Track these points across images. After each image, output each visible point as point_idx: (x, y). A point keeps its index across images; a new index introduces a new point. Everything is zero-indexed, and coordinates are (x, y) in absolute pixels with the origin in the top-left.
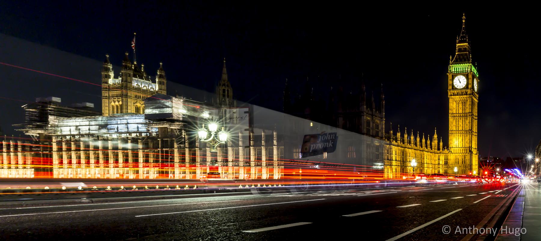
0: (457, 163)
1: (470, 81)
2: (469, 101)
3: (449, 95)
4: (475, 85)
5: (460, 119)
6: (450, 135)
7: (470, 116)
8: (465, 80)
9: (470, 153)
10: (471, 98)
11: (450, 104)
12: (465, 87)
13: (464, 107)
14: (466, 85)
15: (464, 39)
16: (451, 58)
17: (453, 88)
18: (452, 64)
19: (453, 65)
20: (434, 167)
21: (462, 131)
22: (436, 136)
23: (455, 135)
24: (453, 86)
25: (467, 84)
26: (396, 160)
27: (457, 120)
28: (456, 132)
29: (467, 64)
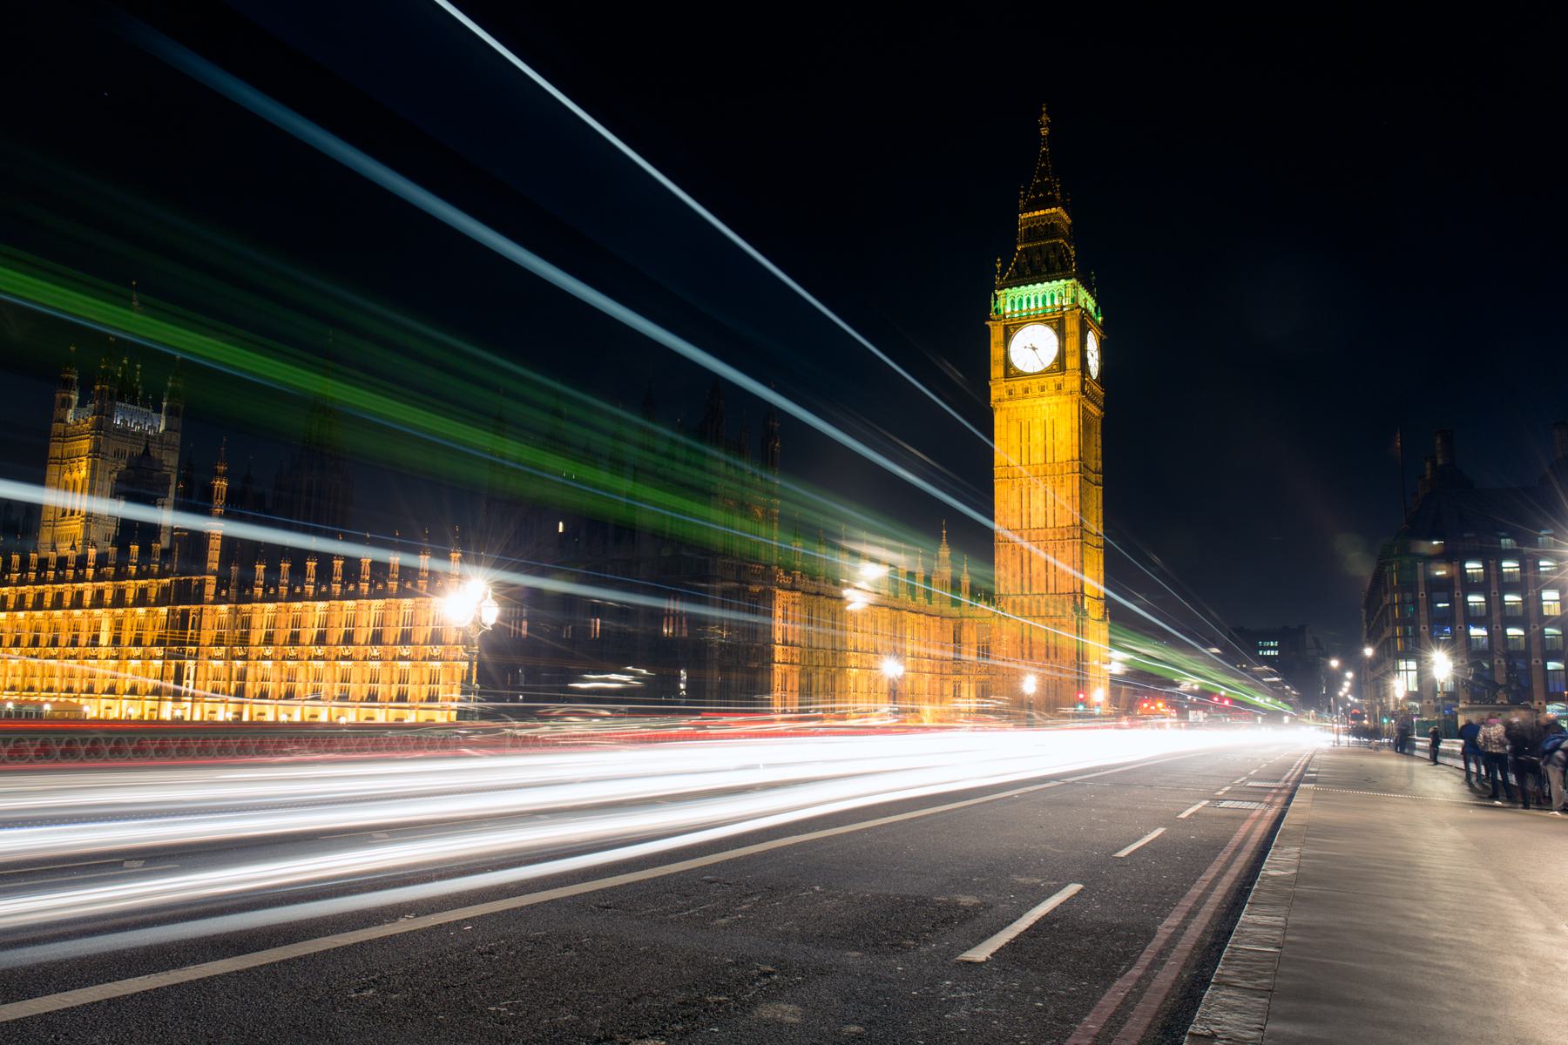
0: (1026, 656)
1: (1072, 343)
3: (993, 398)
4: (1089, 355)
6: (998, 546)
12: (1052, 365)
13: (1049, 438)
14: (1056, 360)
15: (1045, 194)
16: (999, 266)
17: (1010, 371)
19: (1007, 290)
20: (938, 671)
24: (1008, 364)
25: (1059, 352)
26: (785, 643)
27: (1025, 492)
29: (1058, 280)
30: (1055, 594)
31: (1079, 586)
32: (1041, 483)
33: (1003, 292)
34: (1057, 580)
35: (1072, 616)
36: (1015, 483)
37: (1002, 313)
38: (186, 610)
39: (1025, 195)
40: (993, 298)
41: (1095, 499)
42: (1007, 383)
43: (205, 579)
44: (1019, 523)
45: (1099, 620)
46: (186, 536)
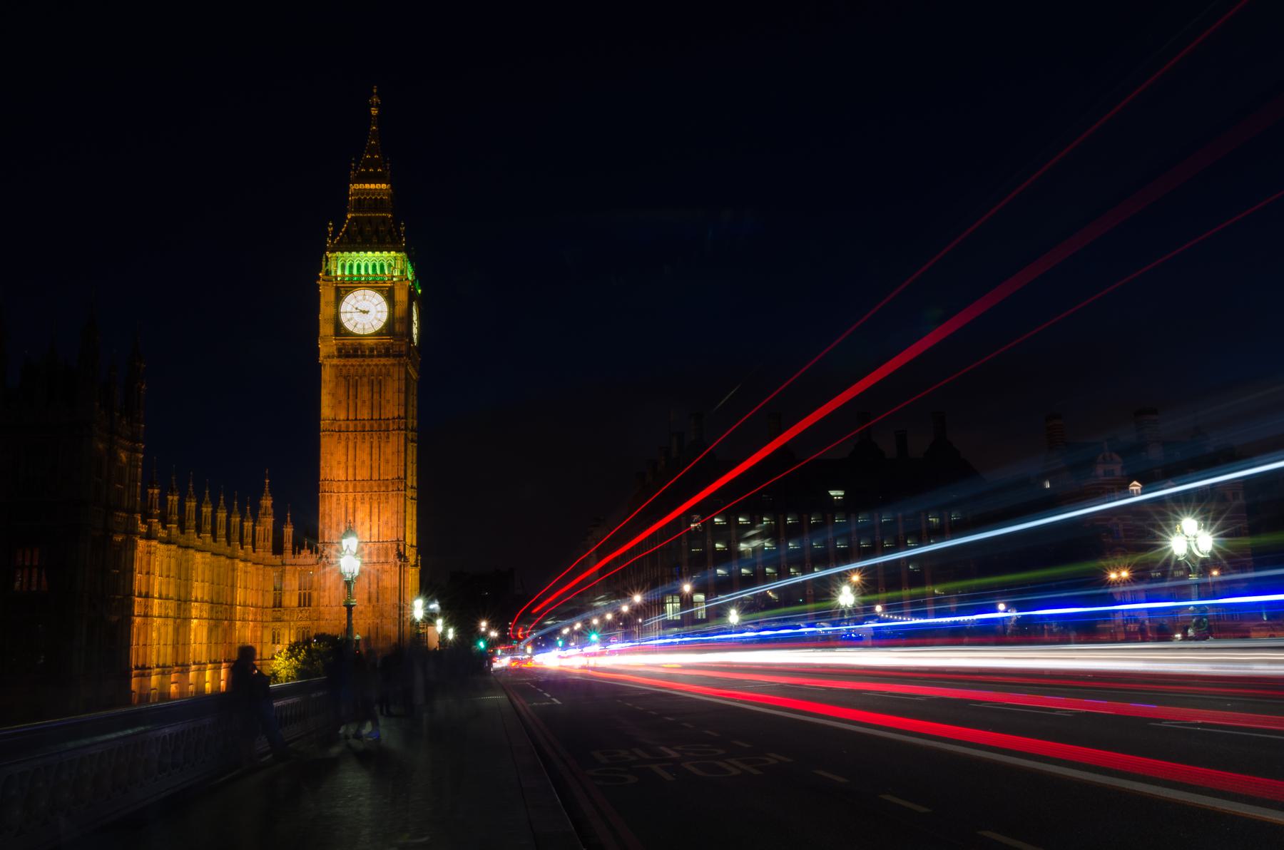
2: (396, 377)
3: (322, 354)
5: (364, 438)
8: (384, 307)
9: (399, 563)
10: (403, 370)
12: (381, 329)
16: (330, 229)
18: (333, 251)
19: (339, 254)
20: (259, 618)
22: (267, 502)
23: (342, 497)
27: (351, 445)
28: (347, 487)
29: (389, 251)
30: (379, 542)
31: (402, 534)
32: (367, 437)
33: (334, 255)
34: (381, 530)
36: (342, 437)
37: (333, 274)
39: (356, 169)
40: (324, 260)
44: (345, 475)
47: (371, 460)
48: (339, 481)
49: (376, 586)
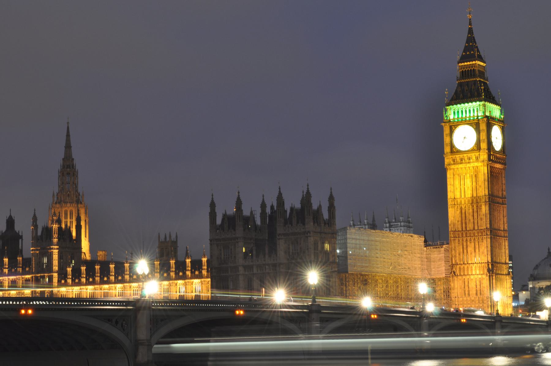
0: (467, 295)
1: (483, 136)
3: (446, 163)
7: (485, 202)
11: (448, 180)
13: (474, 184)
17: (454, 150)
18: (448, 105)
19: (451, 106)
21: (473, 231)
24: (452, 146)
25: (477, 140)
28: (462, 234)
29: (476, 102)
35: (487, 275)
38: (43, 291)
41: (502, 212)
42: (452, 156)
43: (53, 275)
44: (461, 228)
45: (506, 275)
46: (38, 253)
47: (474, 219)
48: (458, 231)
49: (479, 287)
